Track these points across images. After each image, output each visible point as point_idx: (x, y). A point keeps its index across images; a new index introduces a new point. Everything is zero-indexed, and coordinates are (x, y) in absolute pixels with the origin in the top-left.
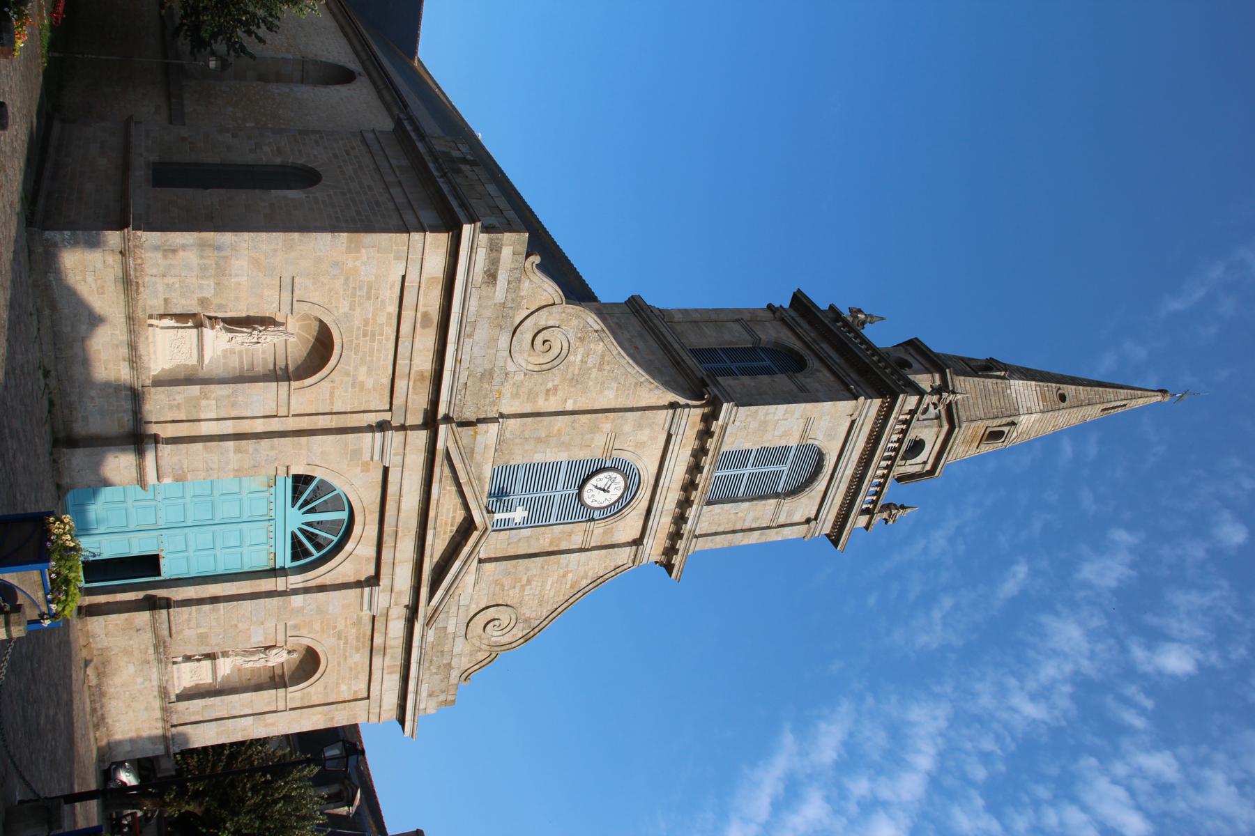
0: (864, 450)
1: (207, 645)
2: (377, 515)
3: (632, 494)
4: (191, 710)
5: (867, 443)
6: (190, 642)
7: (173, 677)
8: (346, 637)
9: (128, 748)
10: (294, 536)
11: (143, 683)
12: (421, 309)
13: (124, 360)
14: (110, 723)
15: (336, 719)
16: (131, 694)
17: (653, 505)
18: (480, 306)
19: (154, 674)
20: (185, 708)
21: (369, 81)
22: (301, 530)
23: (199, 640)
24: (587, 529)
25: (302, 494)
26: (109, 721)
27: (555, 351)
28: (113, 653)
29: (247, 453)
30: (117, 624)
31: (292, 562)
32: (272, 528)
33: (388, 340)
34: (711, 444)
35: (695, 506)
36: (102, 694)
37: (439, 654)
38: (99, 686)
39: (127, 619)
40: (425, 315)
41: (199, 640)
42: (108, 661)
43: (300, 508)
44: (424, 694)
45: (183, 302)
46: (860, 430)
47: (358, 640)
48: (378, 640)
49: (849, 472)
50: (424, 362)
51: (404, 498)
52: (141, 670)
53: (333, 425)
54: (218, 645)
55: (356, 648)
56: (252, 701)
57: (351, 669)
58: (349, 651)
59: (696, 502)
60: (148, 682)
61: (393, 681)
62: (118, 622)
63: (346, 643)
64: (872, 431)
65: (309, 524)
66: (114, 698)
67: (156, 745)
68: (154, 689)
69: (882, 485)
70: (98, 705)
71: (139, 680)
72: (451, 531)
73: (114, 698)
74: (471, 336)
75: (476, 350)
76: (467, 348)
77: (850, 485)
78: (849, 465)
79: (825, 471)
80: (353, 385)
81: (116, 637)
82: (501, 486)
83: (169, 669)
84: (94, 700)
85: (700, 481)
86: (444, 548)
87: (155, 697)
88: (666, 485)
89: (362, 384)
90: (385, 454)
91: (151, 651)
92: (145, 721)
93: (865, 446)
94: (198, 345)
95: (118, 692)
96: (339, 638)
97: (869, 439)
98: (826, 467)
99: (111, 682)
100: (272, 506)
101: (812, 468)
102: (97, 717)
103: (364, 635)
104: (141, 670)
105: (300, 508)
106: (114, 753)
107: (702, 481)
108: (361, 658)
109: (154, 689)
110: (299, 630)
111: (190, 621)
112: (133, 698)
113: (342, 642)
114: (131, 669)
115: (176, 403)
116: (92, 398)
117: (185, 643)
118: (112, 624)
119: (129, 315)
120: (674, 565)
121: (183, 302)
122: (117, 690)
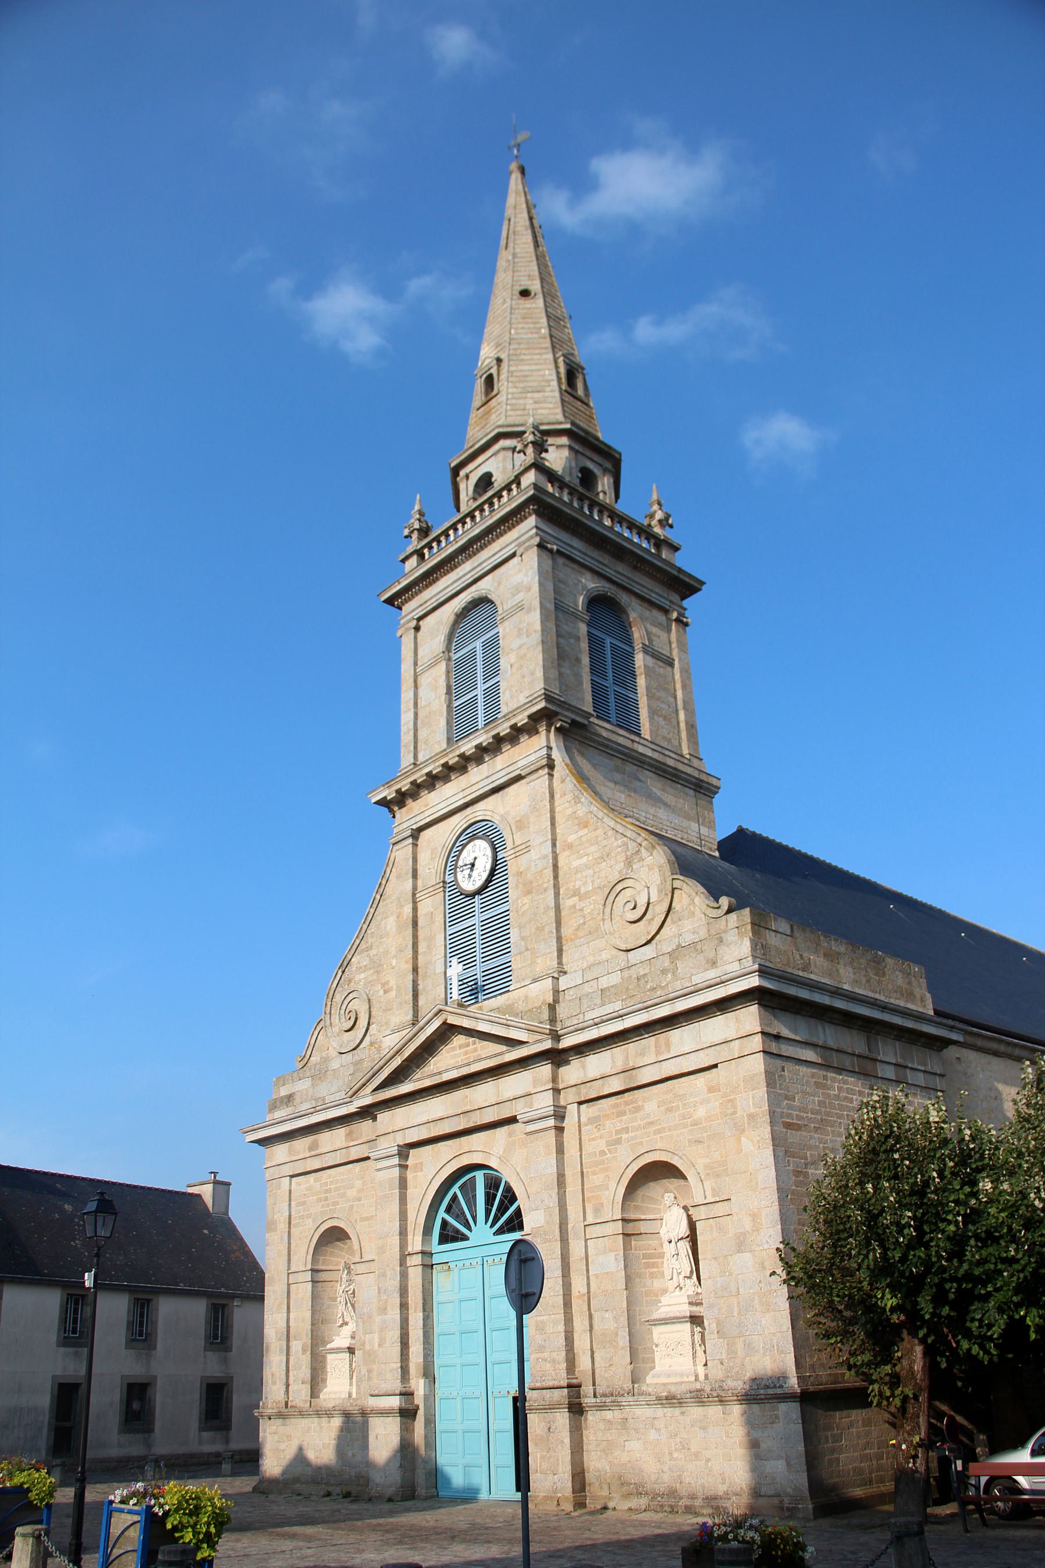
0: (445, 575)
1: (617, 1335)
2: (464, 1140)
3: (485, 823)
4: (724, 1356)
5: (437, 579)
6: (611, 1359)
7: (664, 1384)
8: (617, 1132)
9: (777, 1467)
10: (496, 1233)
11: (658, 1430)
12: (308, 1154)
13: (329, 1422)
14: (725, 1489)
15: (752, 1110)
16: (676, 1450)
17: (511, 779)
18: (306, 1100)
19: (643, 1412)
20: (720, 1366)
21: (1011, 1061)
22: (492, 1226)
23: (608, 1345)
24: (514, 856)
25: (458, 1231)
26: (721, 1489)
27: (621, 900)
28: (608, 1467)
29: (387, 1300)
30: (542, 1457)
31: (439, 1244)
32: (490, 1259)
33: (330, 1176)
34: (452, 759)
35: (462, 750)
36: (672, 1493)
37: (642, 982)
38: (655, 1496)
39: (536, 1445)
40: (310, 1149)
41: (608, 1345)
42: (620, 1478)
43: (470, 1229)
44: (712, 974)
45: (304, 1367)
46: (426, 602)
47: (624, 1113)
48: (615, 1085)
49: (467, 566)
50: (336, 1137)
51: (714, 1040)
52: (637, 1430)
53: (568, 1172)
54: (616, 1319)
55: (634, 1113)
56: (715, 1258)
57: (670, 1110)
58: (639, 1122)
59: (458, 753)
60: (656, 1422)
61: (682, 1037)
62: (538, 1455)
63: (626, 1130)
64: (427, 587)
65: (488, 1212)
66: (680, 1476)
67: (777, 1417)
68: (669, 1414)
69: (446, 533)
70: (683, 1502)
71: (653, 1435)
72: (474, 1043)
73: (680, 1476)
74: (324, 1099)
75: (333, 1090)
76: (331, 1098)
77: (478, 551)
78: (461, 574)
79: (470, 596)
80: (360, 1199)
81: (558, 1460)
82: (468, 994)
83: (650, 1390)
84: (671, 1506)
85: (438, 766)
86: (491, 1044)
87: (683, 1413)
88: (461, 795)
89: (360, 1191)
90: (389, 1154)
91: (608, 1415)
92: (727, 1433)
93: (442, 577)
94: (337, 1353)
95: (670, 1469)
96: (618, 1141)
97: (434, 581)
98: (473, 595)
99: (653, 1478)
100: (474, 1262)
101: (473, 614)
102: (702, 1507)
103: (616, 1106)
104: (637, 1430)
105: (470, 1229)
106: (789, 1490)
107: (451, 756)
108: (651, 1101)
109: (669, 1414)
110: (602, 1204)
111: (554, 1360)
112: (684, 1446)
113: (624, 1136)
114: (635, 1445)
115: (367, 1374)
116: (353, 1455)
117: (611, 1365)
118: (541, 1463)
119: (739, 1400)
120: (529, 717)
121: (304, 1367)
122: (666, 1469)
